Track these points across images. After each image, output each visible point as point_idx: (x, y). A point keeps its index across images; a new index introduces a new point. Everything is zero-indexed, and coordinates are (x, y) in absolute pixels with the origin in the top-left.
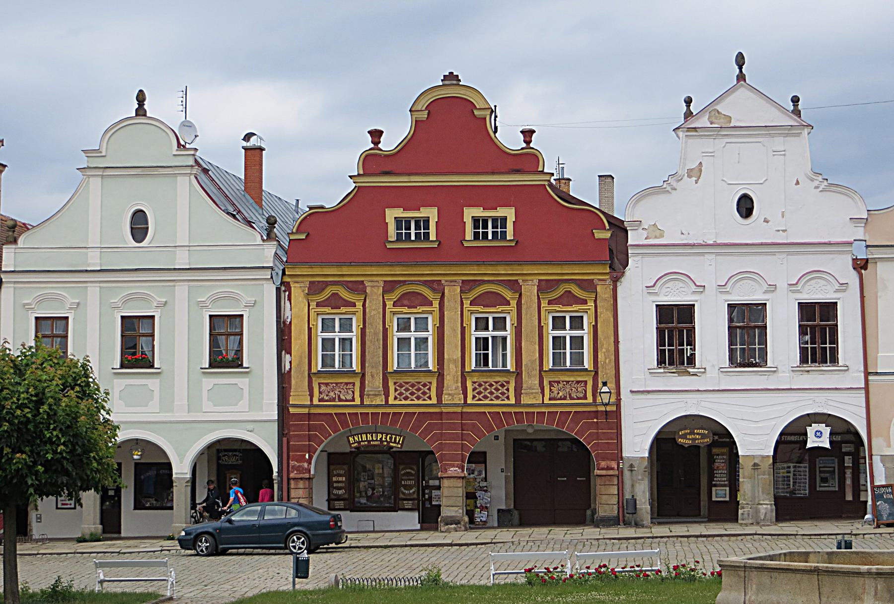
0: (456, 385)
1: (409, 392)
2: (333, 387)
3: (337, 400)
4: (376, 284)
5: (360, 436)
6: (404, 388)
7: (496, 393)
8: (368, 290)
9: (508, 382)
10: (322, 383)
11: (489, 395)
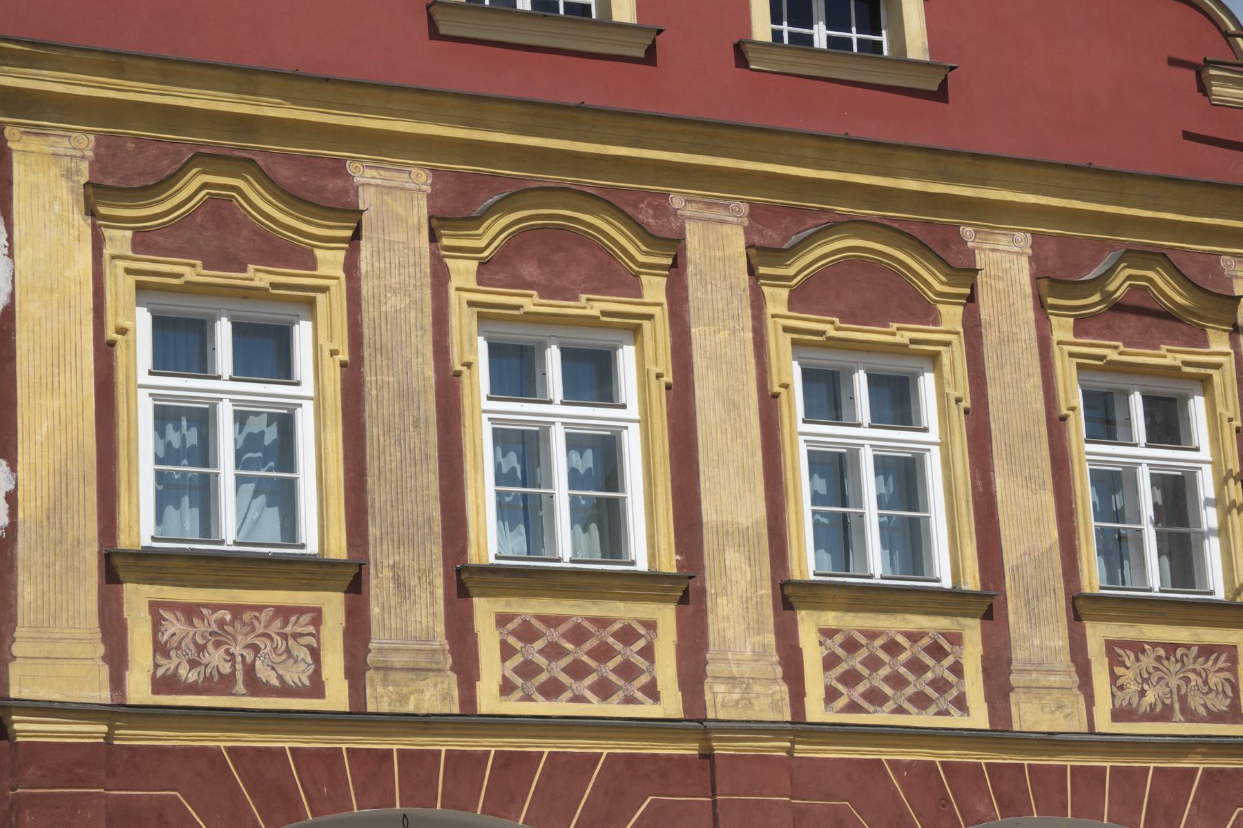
0: (757, 639)
1: (564, 662)
3: (240, 687)
6: (539, 644)
9: (956, 639)
10: (171, 606)
11: (888, 690)
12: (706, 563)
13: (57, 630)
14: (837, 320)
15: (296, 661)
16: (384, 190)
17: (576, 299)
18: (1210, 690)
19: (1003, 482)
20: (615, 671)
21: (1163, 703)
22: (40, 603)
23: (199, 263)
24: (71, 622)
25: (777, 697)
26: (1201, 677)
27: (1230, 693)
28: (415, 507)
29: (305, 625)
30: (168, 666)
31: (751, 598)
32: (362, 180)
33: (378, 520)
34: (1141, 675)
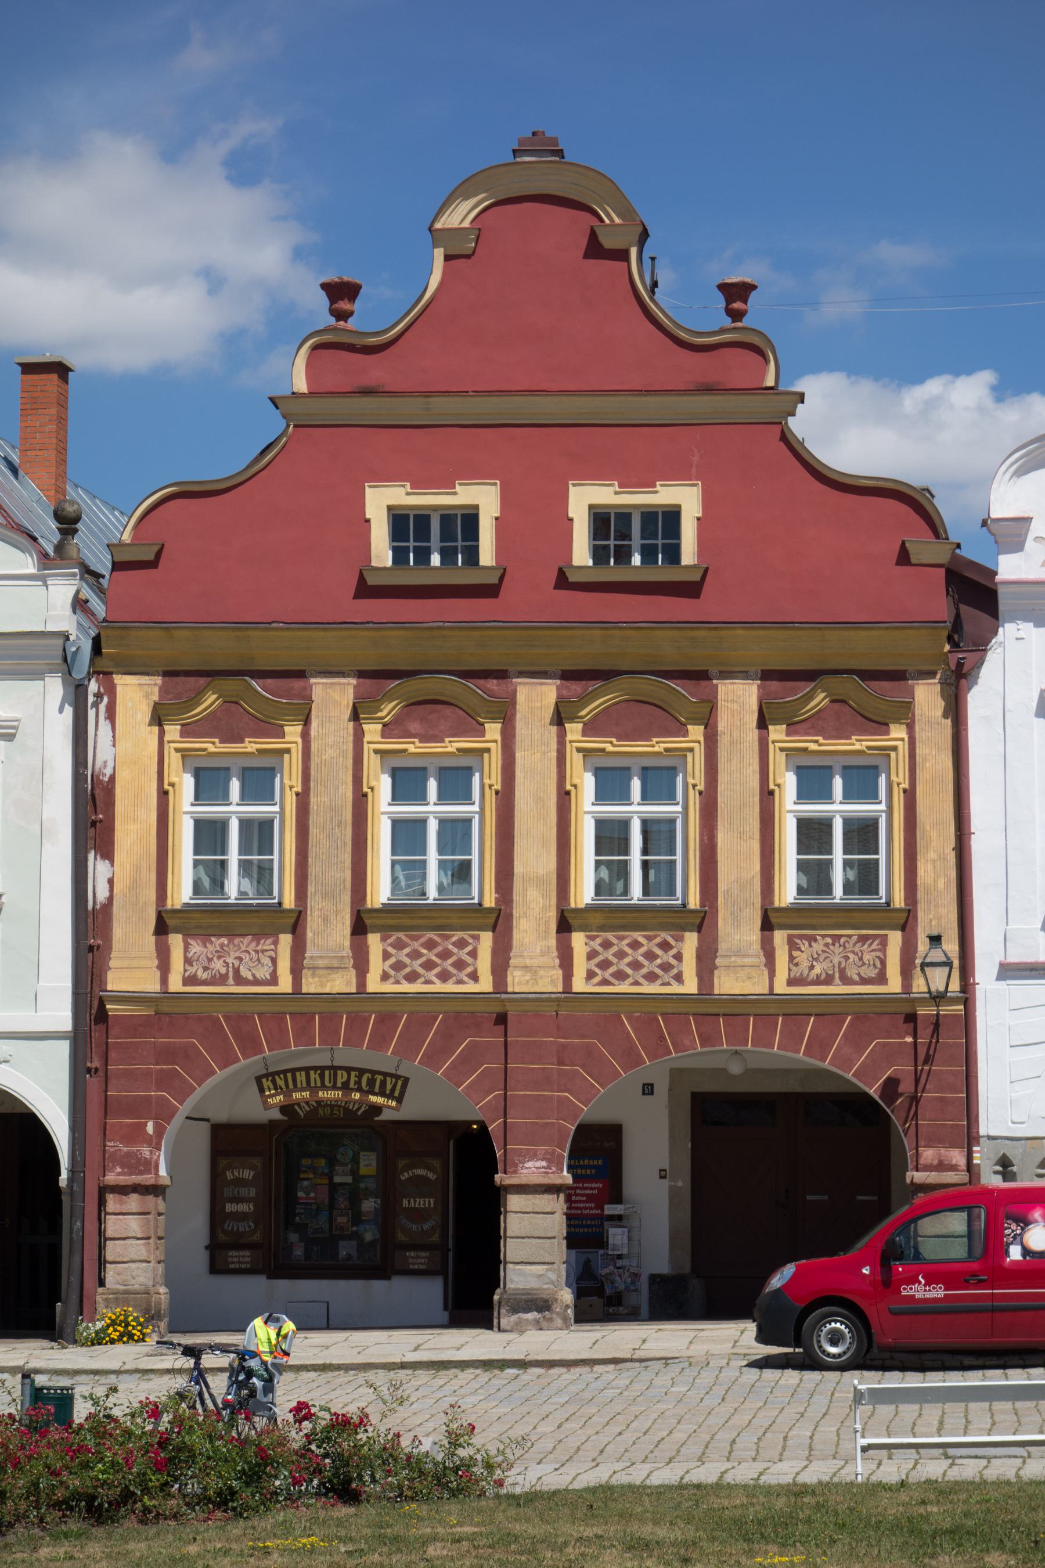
0: (544, 943)
2: (222, 945)
3: (231, 981)
5: (289, 1075)
6: (407, 950)
7: (648, 967)
11: (629, 971)
12: (514, 898)
14: (614, 740)
15: (263, 966)
17: (443, 741)
18: (864, 964)
21: (827, 973)
23: (217, 740)
27: (878, 965)
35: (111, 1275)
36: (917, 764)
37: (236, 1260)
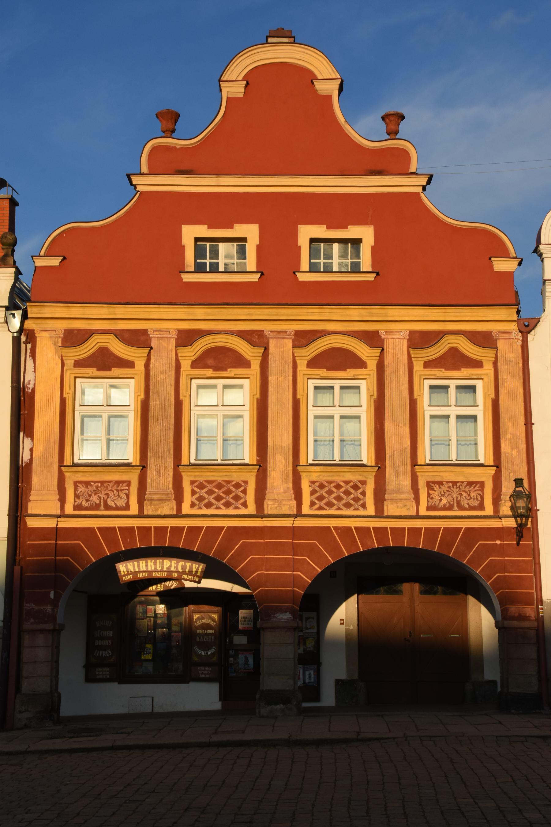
1: (214, 496)
3: (102, 508)
4: (166, 335)
6: (205, 490)
8: (154, 343)
9: (364, 483)
10: (81, 482)
11: (335, 502)
13: (44, 491)
15: (121, 498)
16: (160, 339)
18: (471, 498)
19: (388, 424)
20: (232, 498)
21: (449, 503)
22: (39, 483)
23: (95, 369)
24: (48, 488)
25: (292, 505)
26: (467, 493)
27: (479, 499)
28: (164, 446)
29: (125, 487)
30: (78, 502)
31: (284, 471)
32: (153, 336)
33: (151, 451)
34: (441, 493)
35: (25, 687)
36: (499, 384)
37: (100, 673)
